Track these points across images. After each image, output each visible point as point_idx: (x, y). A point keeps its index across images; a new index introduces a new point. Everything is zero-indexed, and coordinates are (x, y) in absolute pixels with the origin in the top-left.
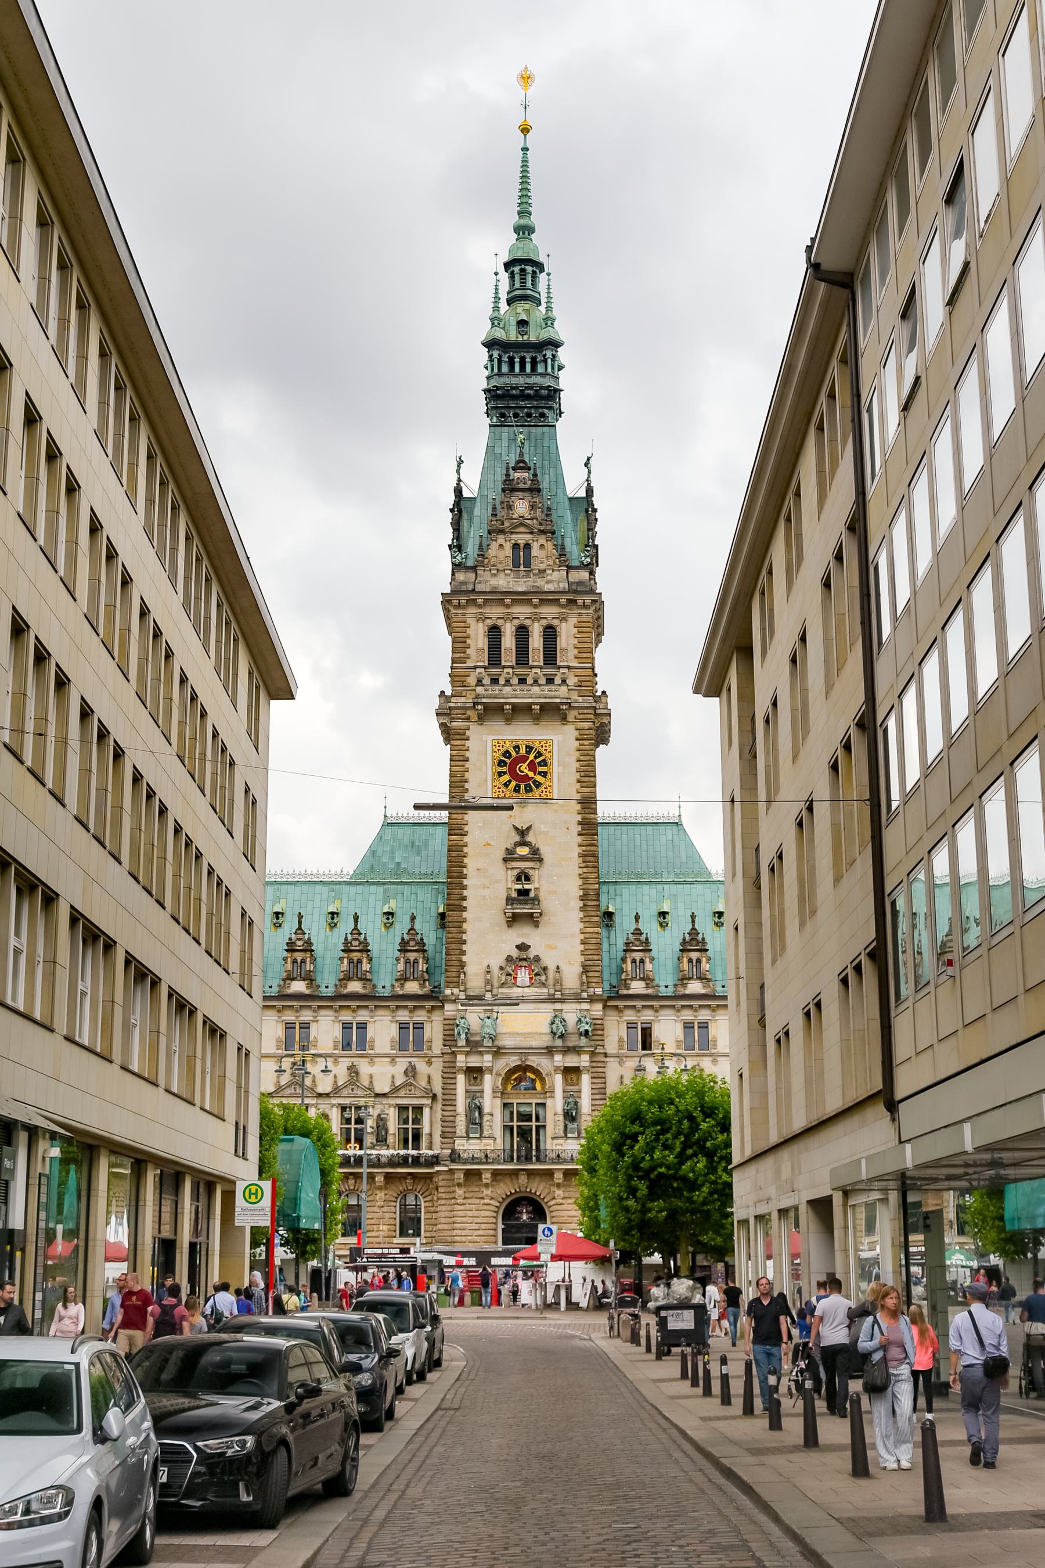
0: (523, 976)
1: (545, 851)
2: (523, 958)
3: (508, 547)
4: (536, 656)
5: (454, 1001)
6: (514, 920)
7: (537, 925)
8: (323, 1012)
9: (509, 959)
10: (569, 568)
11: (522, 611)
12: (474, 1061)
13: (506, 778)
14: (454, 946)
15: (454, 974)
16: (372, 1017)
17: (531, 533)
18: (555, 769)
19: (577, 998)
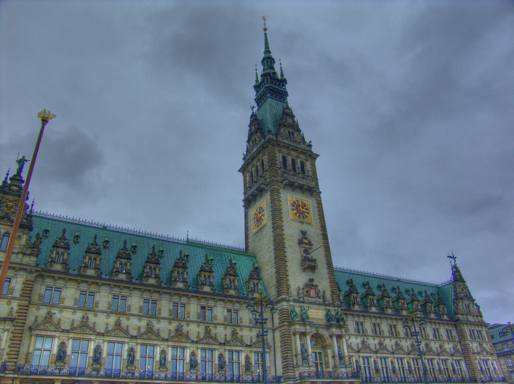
1: (312, 243)
3: (287, 131)
5: (288, 301)
8: (219, 303)
12: (301, 329)
13: (295, 211)
14: (284, 276)
15: (286, 289)
16: (241, 307)
17: (294, 129)
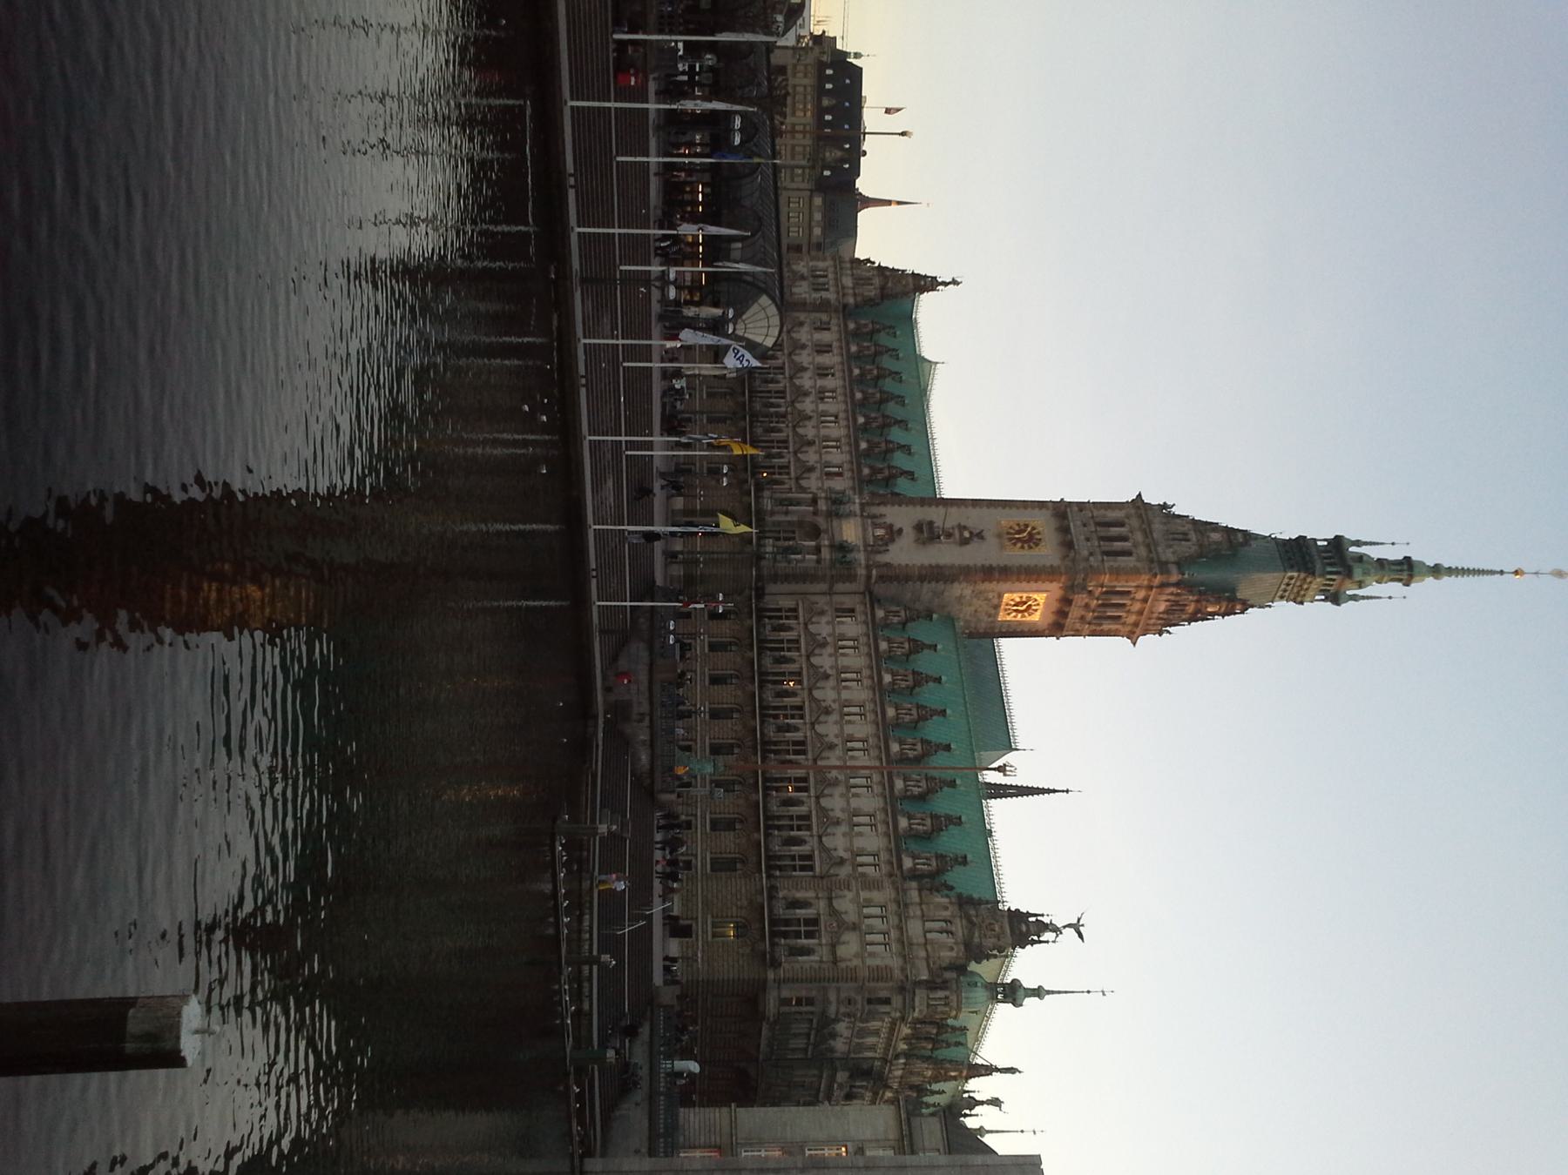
0: (880, 532)
1: (968, 547)
2: (893, 534)
4: (1106, 546)
6: (919, 527)
7: (917, 541)
9: (891, 526)
10: (1178, 564)
11: (1139, 537)
18: (1026, 552)
19: (867, 559)
